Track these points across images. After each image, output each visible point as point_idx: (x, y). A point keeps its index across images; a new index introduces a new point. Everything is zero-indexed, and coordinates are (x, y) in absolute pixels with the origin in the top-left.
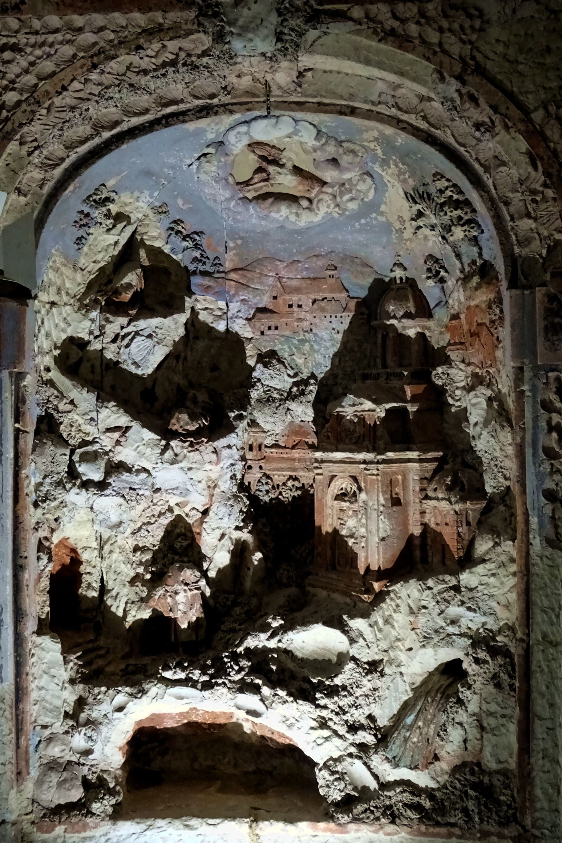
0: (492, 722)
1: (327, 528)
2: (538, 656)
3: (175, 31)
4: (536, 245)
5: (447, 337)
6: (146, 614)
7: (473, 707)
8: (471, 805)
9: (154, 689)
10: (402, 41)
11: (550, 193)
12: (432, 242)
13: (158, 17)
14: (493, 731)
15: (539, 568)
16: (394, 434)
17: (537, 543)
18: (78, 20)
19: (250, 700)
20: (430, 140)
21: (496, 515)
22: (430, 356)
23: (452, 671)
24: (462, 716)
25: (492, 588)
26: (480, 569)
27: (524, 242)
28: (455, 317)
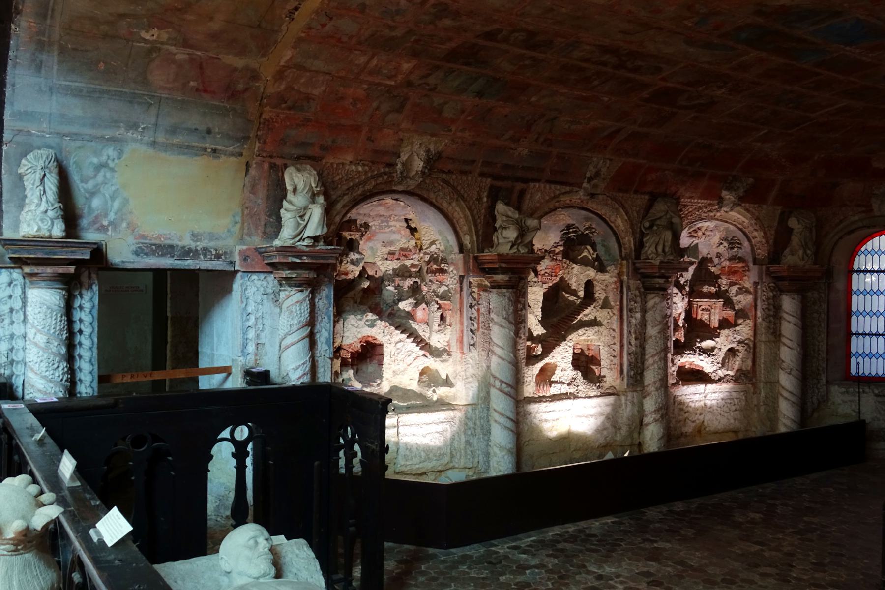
1: (699, 318)
10: (748, 211)
12: (721, 249)
15: (758, 325)
17: (759, 320)
19: (701, 358)
21: (741, 314)
23: (731, 350)
24: (738, 359)
25: (744, 330)
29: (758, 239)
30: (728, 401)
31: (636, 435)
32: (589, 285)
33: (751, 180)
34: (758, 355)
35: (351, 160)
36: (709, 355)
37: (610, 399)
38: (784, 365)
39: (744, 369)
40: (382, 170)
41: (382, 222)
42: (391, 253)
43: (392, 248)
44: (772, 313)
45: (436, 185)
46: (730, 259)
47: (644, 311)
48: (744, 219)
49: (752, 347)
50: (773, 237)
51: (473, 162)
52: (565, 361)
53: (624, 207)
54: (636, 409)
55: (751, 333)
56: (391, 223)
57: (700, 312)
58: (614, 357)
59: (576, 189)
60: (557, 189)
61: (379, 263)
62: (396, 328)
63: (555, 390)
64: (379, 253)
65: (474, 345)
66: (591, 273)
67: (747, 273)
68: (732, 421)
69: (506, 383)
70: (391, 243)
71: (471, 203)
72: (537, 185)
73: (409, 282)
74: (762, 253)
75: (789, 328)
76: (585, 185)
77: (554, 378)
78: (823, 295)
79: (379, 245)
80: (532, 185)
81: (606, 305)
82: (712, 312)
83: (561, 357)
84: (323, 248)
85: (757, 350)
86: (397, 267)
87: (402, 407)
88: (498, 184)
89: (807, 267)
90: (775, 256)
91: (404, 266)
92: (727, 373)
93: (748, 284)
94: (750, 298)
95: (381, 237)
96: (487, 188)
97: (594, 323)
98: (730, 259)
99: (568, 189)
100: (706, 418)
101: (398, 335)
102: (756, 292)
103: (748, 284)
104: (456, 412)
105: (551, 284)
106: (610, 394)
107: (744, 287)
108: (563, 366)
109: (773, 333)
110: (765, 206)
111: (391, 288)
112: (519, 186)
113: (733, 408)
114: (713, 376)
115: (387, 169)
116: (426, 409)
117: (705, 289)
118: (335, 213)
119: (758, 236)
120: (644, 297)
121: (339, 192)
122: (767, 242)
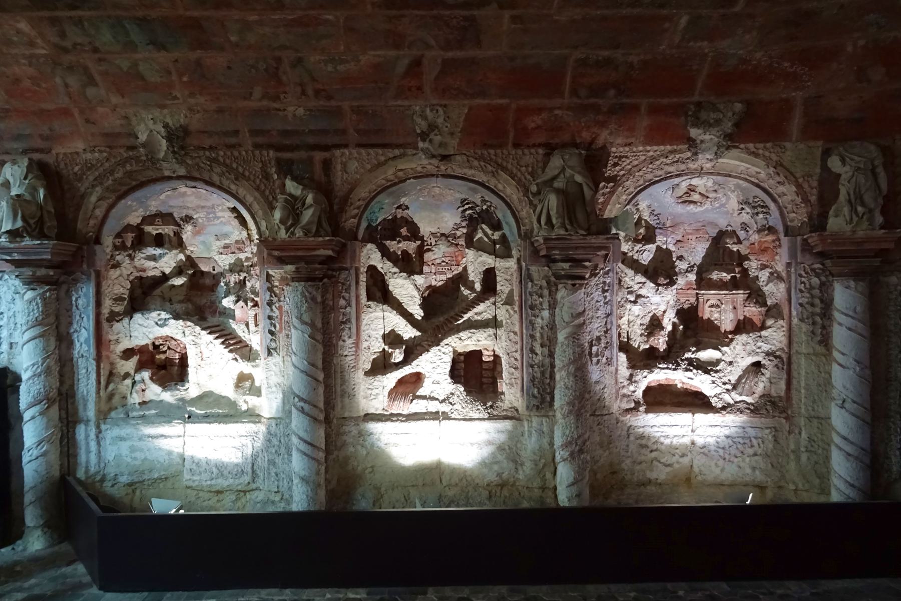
0: (775, 380)
1: (705, 317)
2: (794, 358)
3: (680, 152)
4: (796, 222)
5: (748, 251)
6: (647, 346)
7: (768, 376)
8: (768, 407)
9: (657, 371)
10: (756, 155)
11: (803, 205)
12: (745, 217)
13: (675, 147)
14: (775, 383)
15: (795, 328)
16: (734, 285)
17: (795, 321)
18: (648, 148)
19: (689, 374)
20: (758, 186)
21: (773, 312)
22: (741, 259)
23: (757, 365)
24: (764, 379)
25: (775, 336)
26: (770, 330)
27: (792, 221)
28: (753, 244)
29: (789, 198)
30: (737, 444)
31: (549, 476)
32: (489, 276)
33: (738, 107)
34: (794, 374)
35: (83, 147)
36: (707, 372)
37: (507, 425)
38: (835, 393)
39: (773, 393)
40: (125, 155)
41: (208, 213)
42: (226, 247)
43: (227, 242)
44: (818, 310)
45: (202, 165)
46: (759, 231)
47: (552, 307)
48: (755, 169)
49: (785, 361)
50: (815, 191)
51: (236, 133)
52: (439, 370)
53: (504, 169)
54: (546, 441)
55: (785, 340)
56: (219, 214)
57: (707, 309)
58: (516, 368)
59: (410, 151)
60: (381, 154)
61: (216, 258)
62: (203, 329)
63: (418, 406)
64: (214, 248)
65: (275, 349)
66: (489, 261)
67: (779, 250)
68: (749, 471)
69: (298, 396)
70: (226, 235)
71: (258, 181)
72: (347, 152)
73: (233, 279)
74: (798, 217)
75: (842, 336)
76: (421, 145)
77: (421, 392)
79: (212, 239)
80: (338, 153)
81: (509, 302)
82: (723, 310)
83: (435, 365)
84: (28, 243)
85: (794, 366)
86: (232, 261)
87: (198, 416)
88: (287, 155)
89: (860, 234)
90: (818, 223)
91: (239, 259)
92: (739, 398)
93: (780, 267)
94: (782, 286)
95: (213, 229)
96: (273, 163)
97: (494, 323)
98: (759, 231)
99: (397, 152)
100: (696, 463)
101: (206, 337)
102: (789, 276)
103: (780, 267)
104: (259, 425)
105: (449, 276)
106: (505, 418)
107: (776, 272)
108: (435, 377)
109: (820, 342)
110: (788, 145)
111: (222, 284)
112: (319, 156)
113: (750, 451)
114: (713, 401)
115: (131, 153)
116: (226, 419)
117: (715, 276)
118: (91, 207)
119: (788, 192)
120: (552, 288)
121: (86, 184)
122: (806, 200)
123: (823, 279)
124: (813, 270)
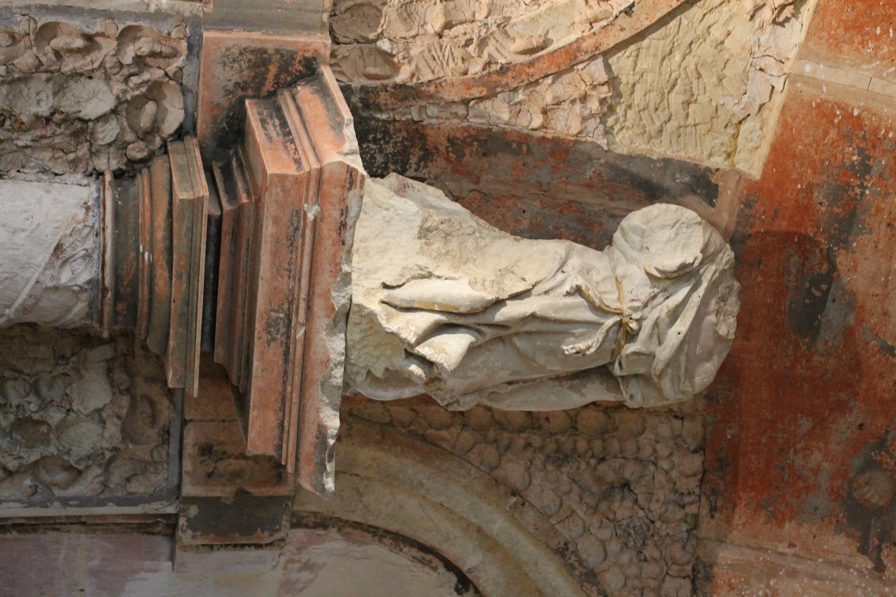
4: (399, 30)
11: (475, 68)
78: (86, 486)
122: (497, 80)
123: (108, 133)
124: (154, 91)
